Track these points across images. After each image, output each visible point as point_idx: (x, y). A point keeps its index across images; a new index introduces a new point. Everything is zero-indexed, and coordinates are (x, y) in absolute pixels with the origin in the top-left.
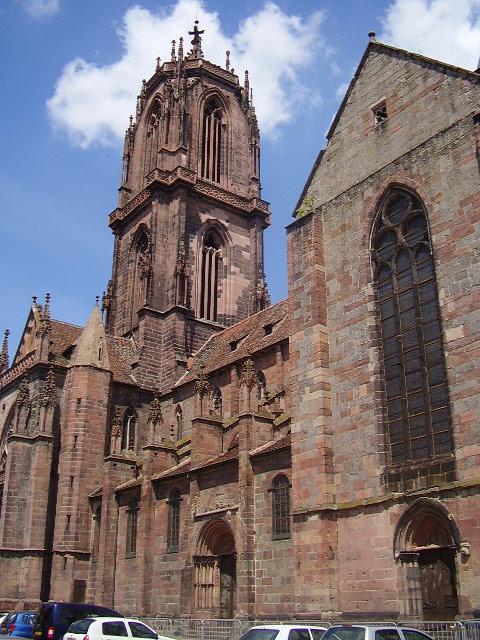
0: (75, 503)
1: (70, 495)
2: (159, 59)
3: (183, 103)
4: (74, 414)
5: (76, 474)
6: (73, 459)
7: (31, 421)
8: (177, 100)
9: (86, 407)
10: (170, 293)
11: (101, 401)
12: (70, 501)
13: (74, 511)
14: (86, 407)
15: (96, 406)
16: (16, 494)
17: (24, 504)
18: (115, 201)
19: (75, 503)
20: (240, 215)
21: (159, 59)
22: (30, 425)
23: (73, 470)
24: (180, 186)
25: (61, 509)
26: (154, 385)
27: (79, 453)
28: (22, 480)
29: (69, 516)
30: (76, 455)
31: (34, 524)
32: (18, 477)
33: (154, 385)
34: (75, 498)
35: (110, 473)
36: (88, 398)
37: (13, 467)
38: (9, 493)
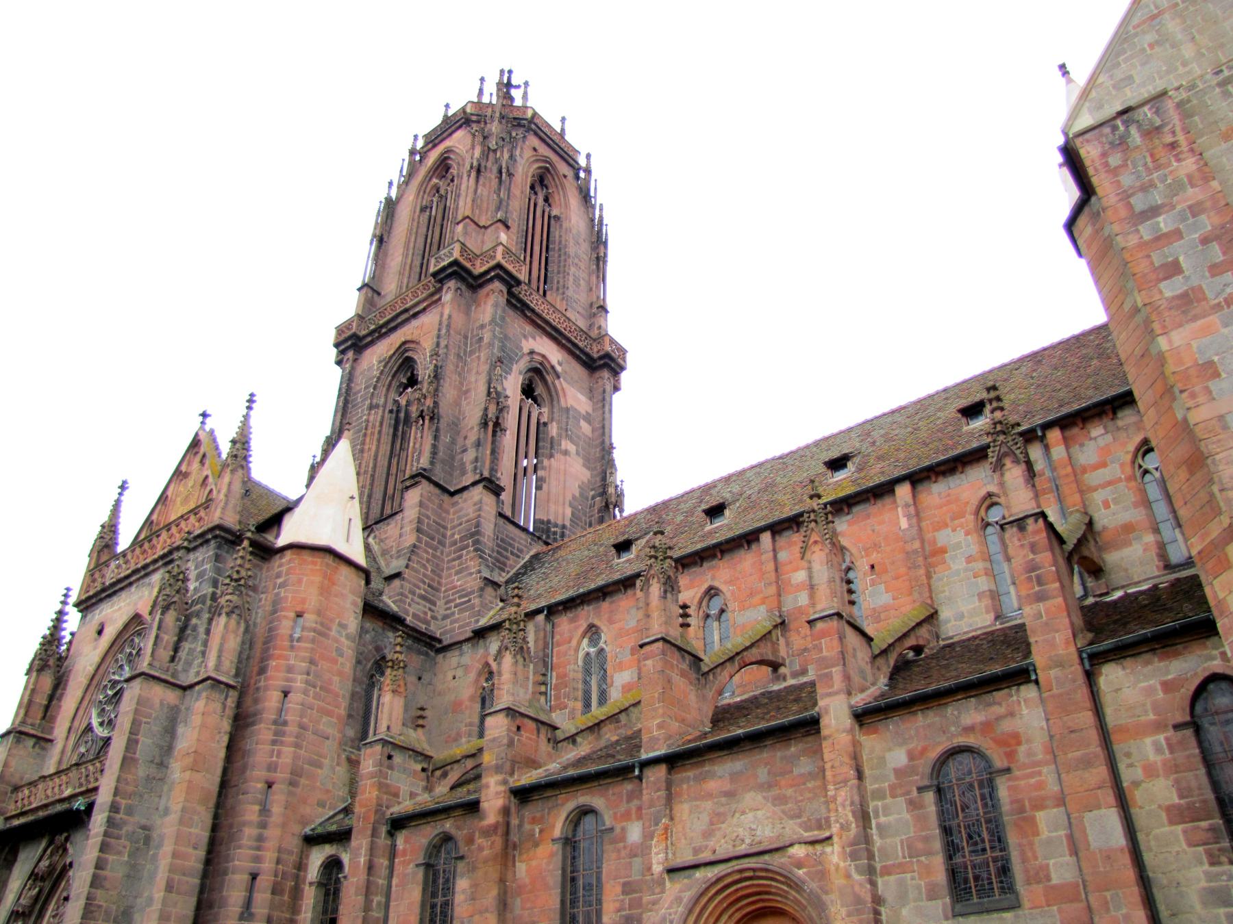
0: (271, 844)
1: (263, 825)
2: (447, 106)
3: (506, 156)
4: (287, 644)
5: (281, 776)
6: (274, 742)
7: (186, 646)
8: (495, 151)
9: (314, 630)
10: (470, 455)
11: (343, 626)
12: (260, 838)
13: (267, 865)
14: (314, 630)
15: (333, 633)
16: (130, 811)
17: (146, 839)
18: (347, 306)
19: (271, 844)
20: (577, 358)
21: (447, 106)
22: (182, 654)
23: (272, 767)
24: (498, 277)
25: (240, 861)
26: (427, 623)
27: (292, 729)
28: (149, 779)
29: (254, 877)
30: (283, 734)
31: (169, 888)
32: (142, 771)
33: (427, 623)
34: (273, 833)
35: (381, 774)
36: (319, 613)
37: (132, 743)
38: (114, 808)
